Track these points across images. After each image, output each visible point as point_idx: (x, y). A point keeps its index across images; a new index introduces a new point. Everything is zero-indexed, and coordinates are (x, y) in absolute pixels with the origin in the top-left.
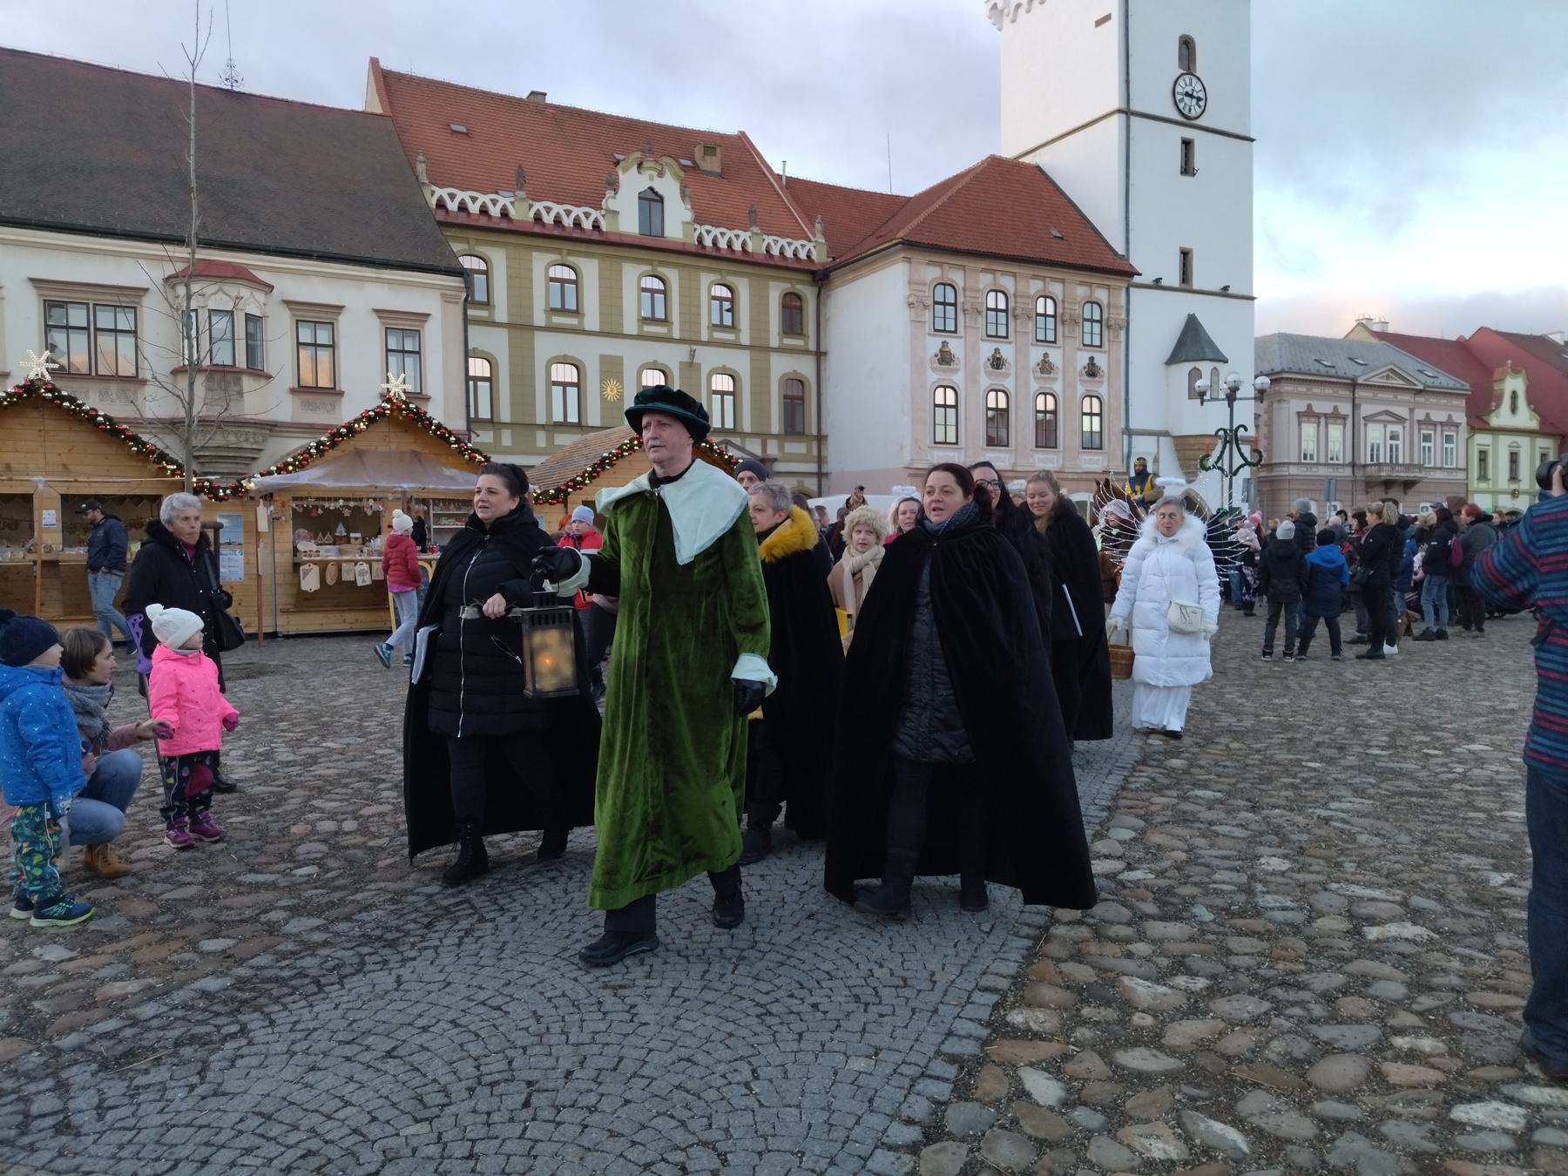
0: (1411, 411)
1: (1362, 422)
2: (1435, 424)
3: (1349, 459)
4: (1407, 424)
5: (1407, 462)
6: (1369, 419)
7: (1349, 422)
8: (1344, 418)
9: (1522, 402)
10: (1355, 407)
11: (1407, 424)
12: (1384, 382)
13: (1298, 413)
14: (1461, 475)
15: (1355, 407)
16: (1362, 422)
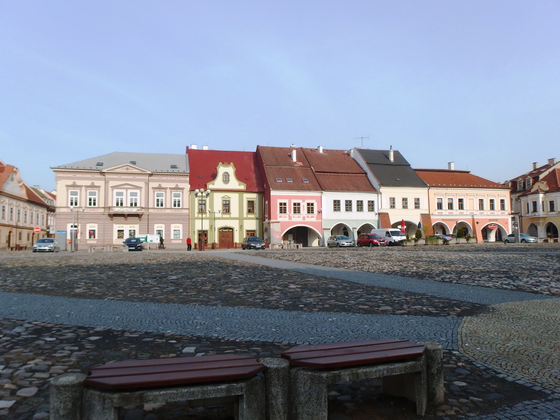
0: (147, 184)
1: (110, 189)
2: (165, 189)
3: (102, 205)
4: (143, 190)
5: (143, 206)
6: (114, 187)
7: (102, 190)
8: (99, 187)
9: (232, 178)
10: (106, 183)
11: (143, 190)
12: (125, 171)
13: (68, 186)
14: (187, 211)
15: (106, 183)
16: (110, 189)
